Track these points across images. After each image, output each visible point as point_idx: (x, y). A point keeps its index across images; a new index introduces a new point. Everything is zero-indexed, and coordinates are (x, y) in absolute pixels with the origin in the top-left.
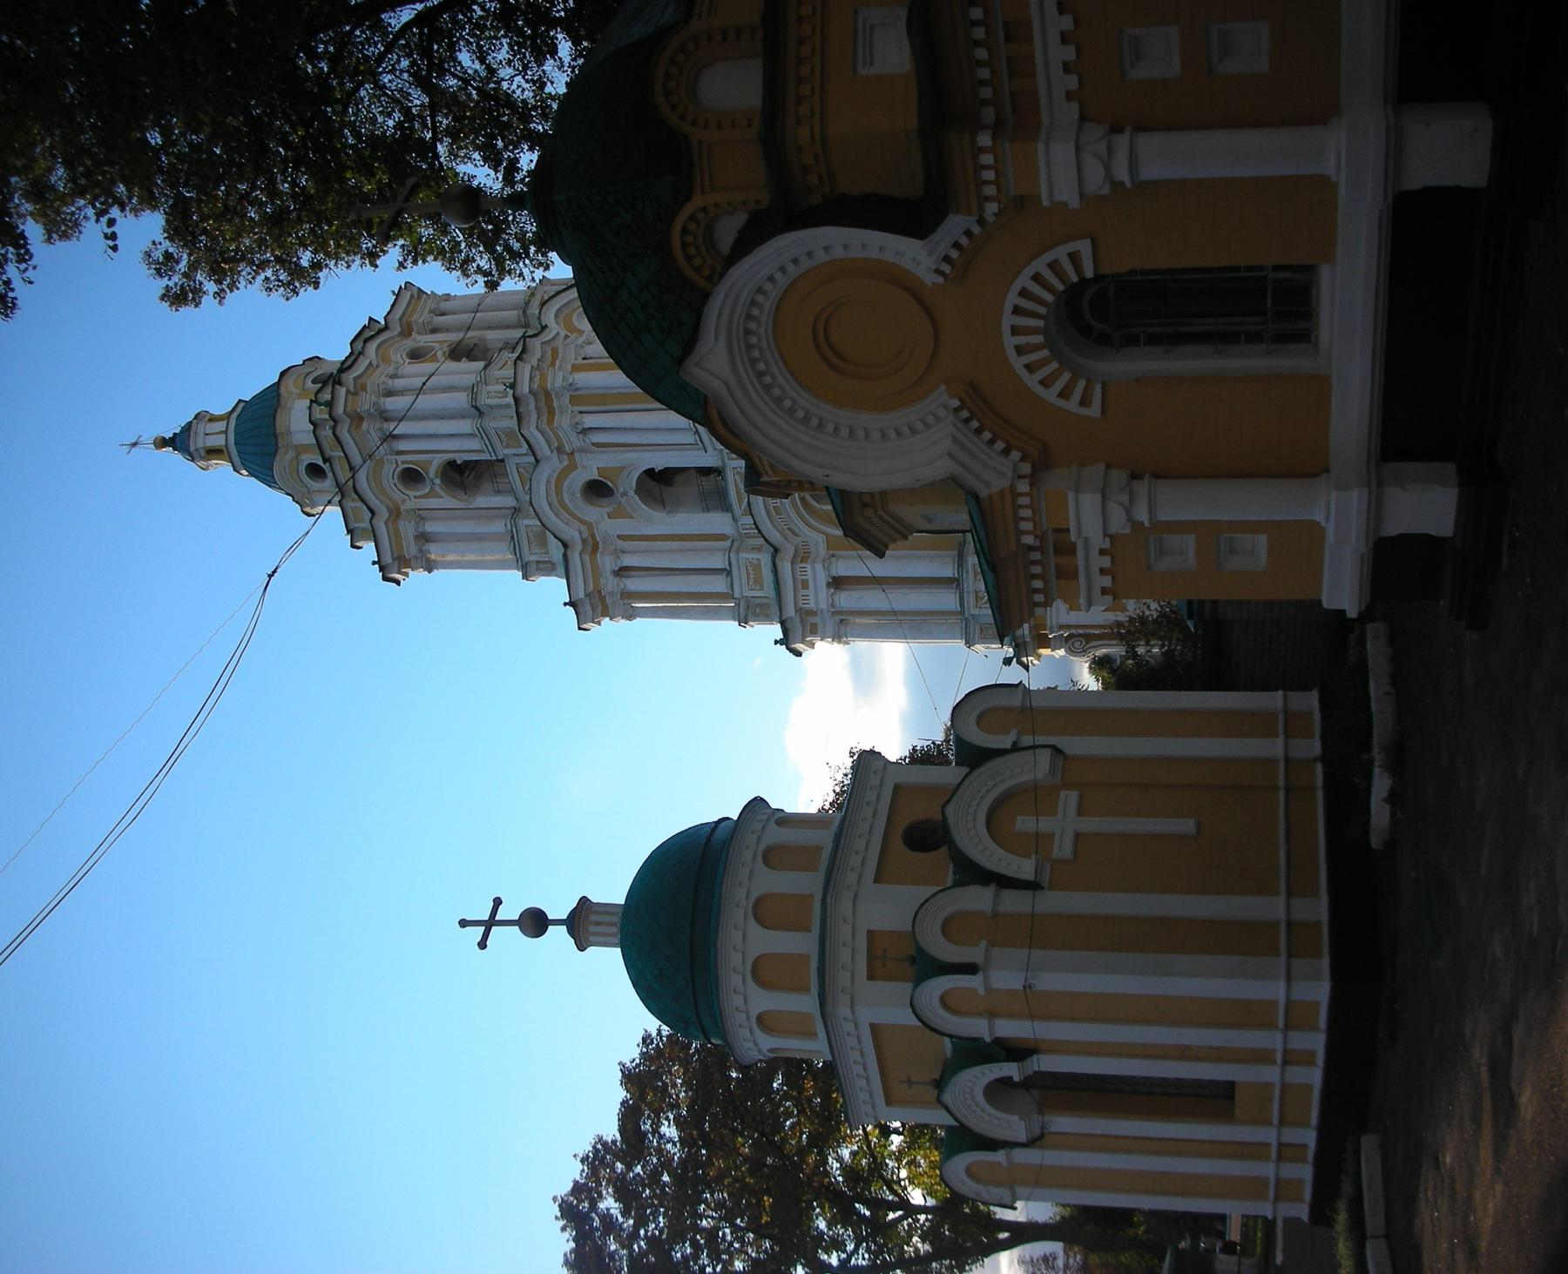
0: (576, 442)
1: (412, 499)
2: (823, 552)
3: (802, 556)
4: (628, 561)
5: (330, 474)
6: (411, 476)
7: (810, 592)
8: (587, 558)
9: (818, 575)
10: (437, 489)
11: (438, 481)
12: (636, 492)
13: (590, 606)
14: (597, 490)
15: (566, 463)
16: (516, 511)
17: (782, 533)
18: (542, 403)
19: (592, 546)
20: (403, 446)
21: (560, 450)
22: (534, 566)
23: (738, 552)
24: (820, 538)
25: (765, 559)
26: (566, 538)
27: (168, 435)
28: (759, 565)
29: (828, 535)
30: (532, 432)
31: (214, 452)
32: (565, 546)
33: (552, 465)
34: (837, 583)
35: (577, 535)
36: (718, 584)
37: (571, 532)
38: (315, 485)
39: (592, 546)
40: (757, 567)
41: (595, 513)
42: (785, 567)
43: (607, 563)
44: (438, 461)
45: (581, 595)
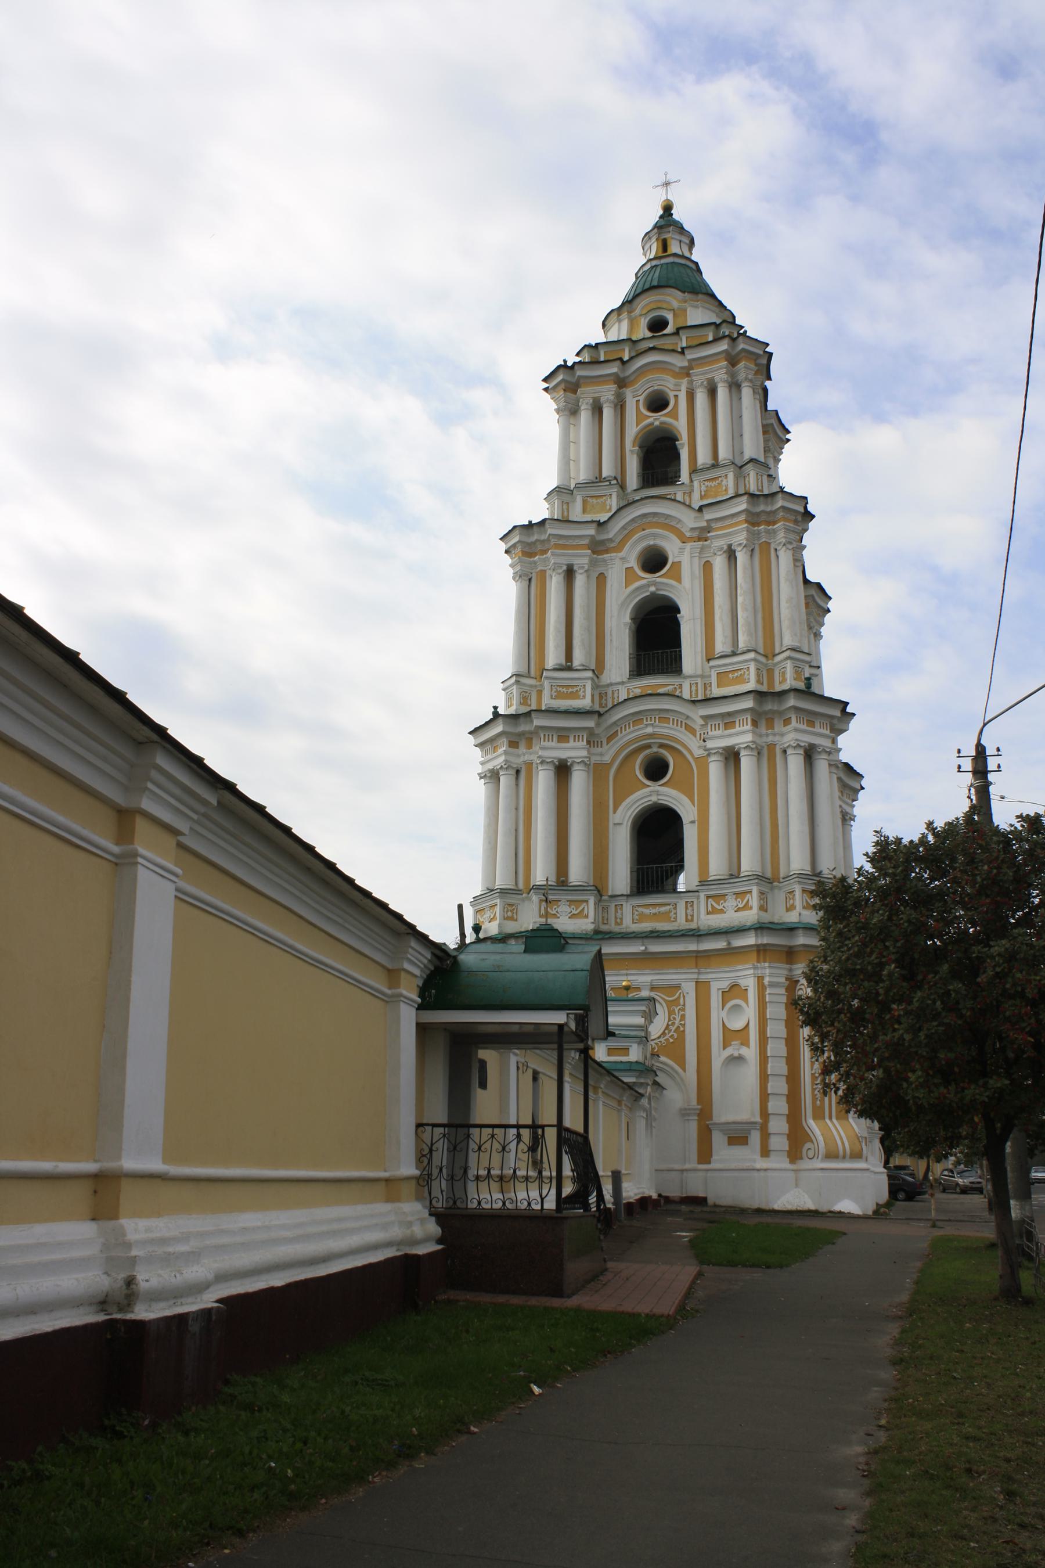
0: (723, 543)
1: (635, 400)
2: (595, 759)
3: (592, 740)
4: (580, 581)
6: (658, 403)
7: (554, 744)
9: (574, 751)
11: (657, 423)
12: (653, 594)
13: (527, 542)
14: (654, 561)
15: (688, 534)
16: (622, 486)
17: (615, 723)
19: (598, 547)
20: (701, 399)
23: (592, 679)
24: (607, 759)
25: (585, 702)
27: (676, 214)
28: (578, 698)
30: (742, 505)
31: (665, 246)
32: (600, 524)
33: (689, 521)
34: (562, 770)
35: (611, 535)
36: (553, 656)
37: (614, 530)
38: (644, 322)
39: (598, 547)
40: (574, 696)
41: (632, 555)
42: (590, 723)
43: (581, 560)
44: (681, 426)
45: (550, 531)
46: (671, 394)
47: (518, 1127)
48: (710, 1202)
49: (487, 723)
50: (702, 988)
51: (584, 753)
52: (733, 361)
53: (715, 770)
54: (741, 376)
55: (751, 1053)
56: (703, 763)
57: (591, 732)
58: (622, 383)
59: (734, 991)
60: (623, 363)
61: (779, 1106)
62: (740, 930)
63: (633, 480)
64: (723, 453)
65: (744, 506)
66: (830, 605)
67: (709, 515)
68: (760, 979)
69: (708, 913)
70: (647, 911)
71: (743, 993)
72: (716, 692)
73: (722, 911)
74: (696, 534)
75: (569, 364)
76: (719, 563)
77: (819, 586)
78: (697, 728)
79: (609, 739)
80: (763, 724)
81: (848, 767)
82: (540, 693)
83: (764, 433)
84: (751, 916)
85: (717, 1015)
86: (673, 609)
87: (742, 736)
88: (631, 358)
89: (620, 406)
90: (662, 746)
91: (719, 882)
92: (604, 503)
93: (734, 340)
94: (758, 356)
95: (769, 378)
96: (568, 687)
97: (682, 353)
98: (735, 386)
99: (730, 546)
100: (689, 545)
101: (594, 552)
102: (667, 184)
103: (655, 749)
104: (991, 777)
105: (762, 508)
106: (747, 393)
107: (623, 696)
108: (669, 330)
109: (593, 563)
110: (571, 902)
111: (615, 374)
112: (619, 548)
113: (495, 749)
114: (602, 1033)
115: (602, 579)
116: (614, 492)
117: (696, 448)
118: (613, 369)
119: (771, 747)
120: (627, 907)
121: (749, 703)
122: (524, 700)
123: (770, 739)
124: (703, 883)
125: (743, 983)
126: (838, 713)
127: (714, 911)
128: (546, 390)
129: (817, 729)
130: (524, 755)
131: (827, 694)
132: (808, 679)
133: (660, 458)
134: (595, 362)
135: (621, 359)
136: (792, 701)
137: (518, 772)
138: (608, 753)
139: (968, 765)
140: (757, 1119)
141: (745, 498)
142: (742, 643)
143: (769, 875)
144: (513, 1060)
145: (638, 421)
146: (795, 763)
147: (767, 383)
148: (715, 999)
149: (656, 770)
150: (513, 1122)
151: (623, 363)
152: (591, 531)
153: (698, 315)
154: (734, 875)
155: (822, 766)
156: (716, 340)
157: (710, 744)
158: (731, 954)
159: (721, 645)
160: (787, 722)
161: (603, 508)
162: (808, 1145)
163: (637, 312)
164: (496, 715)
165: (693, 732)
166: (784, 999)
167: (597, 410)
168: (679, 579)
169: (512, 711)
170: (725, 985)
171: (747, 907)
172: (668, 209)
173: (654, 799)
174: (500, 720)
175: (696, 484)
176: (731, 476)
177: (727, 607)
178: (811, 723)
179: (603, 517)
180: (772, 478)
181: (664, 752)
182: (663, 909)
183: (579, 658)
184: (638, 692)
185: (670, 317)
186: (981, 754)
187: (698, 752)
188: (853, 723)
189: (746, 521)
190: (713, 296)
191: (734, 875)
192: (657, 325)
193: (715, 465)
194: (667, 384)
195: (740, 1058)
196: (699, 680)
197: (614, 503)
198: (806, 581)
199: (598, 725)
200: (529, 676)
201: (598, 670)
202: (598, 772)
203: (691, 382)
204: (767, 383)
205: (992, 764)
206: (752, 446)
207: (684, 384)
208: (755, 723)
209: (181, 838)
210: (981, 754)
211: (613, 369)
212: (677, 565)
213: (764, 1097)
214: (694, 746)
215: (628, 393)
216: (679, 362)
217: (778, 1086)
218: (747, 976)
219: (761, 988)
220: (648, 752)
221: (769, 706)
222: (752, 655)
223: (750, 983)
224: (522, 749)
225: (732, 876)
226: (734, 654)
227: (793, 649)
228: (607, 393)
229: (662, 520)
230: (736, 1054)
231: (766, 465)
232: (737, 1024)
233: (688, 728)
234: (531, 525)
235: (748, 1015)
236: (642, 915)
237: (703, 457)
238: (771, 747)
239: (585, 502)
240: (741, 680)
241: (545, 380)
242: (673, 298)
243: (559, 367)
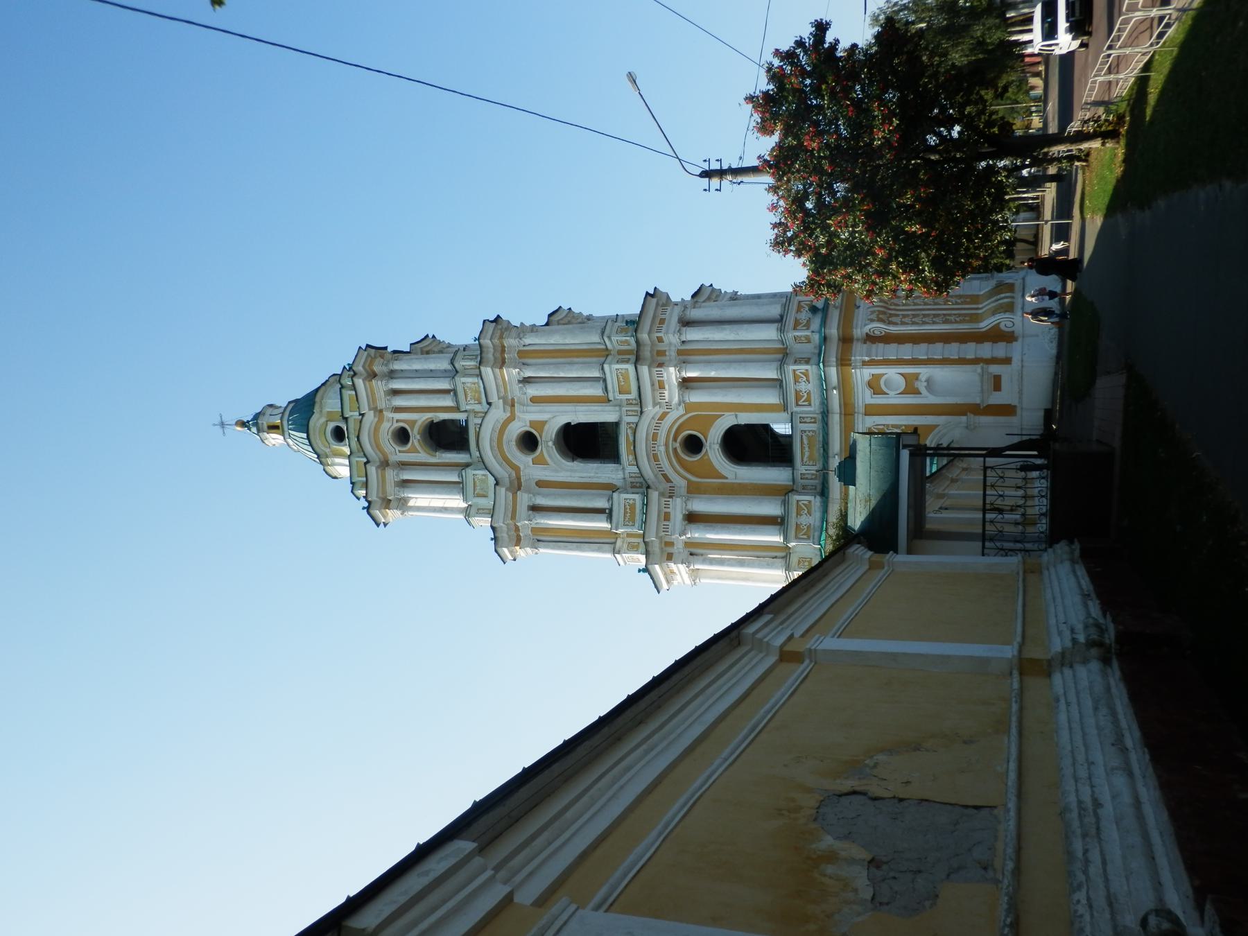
0: (516, 387)
2: (684, 491)
4: (541, 501)
6: (402, 436)
8: (510, 495)
9: (678, 509)
10: (416, 444)
14: (529, 442)
16: (467, 465)
18: (498, 355)
19: (516, 486)
20: (400, 402)
21: (504, 399)
22: (473, 511)
24: (684, 483)
26: (499, 476)
29: (690, 483)
30: (487, 371)
32: (497, 484)
33: (498, 414)
36: (602, 524)
39: (516, 486)
40: (633, 507)
41: (524, 460)
43: (524, 499)
46: (397, 425)
47: (985, 469)
48: (1049, 406)
49: (652, 578)
50: (870, 411)
51: (678, 500)
52: (374, 375)
53: (696, 397)
54: (385, 369)
55: (924, 372)
56: (689, 407)
57: (662, 495)
58: (385, 464)
59: (874, 385)
60: (368, 462)
61: (971, 350)
62: (823, 381)
63: (460, 457)
64: (444, 385)
65: (489, 369)
66: (565, 307)
67: (494, 398)
68: (864, 363)
70: (807, 454)
71: (876, 378)
72: (634, 395)
73: (809, 394)
74: (508, 408)
75: (366, 504)
76: (532, 391)
77: (550, 316)
78: (662, 411)
79: (668, 480)
80: (661, 359)
81: (694, 295)
82: (629, 535)
83: (428, 353)
85: (893, 399)
86: (567, 426)
87: (672, 375)
88: (365, 455)
89: (403, 465)
90: (675, 439)
91: (784, 396)
92: (482, 480)
93: (355, 374)
94: (369, 355)
95: (386, 348)
96: (625, 513)
97: (363, 415)
98: (392, 375)
99: (520, 382)
100: (517, 413)
101: (519, 489)
102: (222, 424)
103: (677, 445)
104: (725, 167)
105: (490, 356)
106: (397, 366)
107: (635, 469)
109: (529, 491)
110: (798, 514)
111: (377, 468)
112: (517, 469)
113: (672, 572)
114: (915, 437)
115: (541, 484)
116: (470, 472)
117: (441, 408)
118: (372, 470)
119: (680, 352)
120: (801, 468)
121: (644, 370)
122: (633, 548)
123: (673, 354)
124: (785, 408)
125: (867, 377)
126: (654, 301)
127: (809, 400)
128: (385, 525)
129: (666, 316)
130: (679, 547)
131: (637, 311)
132: (627, 322)
133: (448, 436)
134: (366, 485)
135: (365, 464)
136: (644, 336)
137: (691, 554)
138: (680, 483)
139: (715, 182)
140: (978, 368)
141: (482, 368)
142: (597, 374)
143: (780, 356)
144: (932, 515)
145: (417, 451)
147: (390, 350)
148: (880, 400)
149: (693, 445)
150: (981, 516)
151: (368, 462)
152: (502, 491)
153: (330, 403)
154: (779, 384)
155: (695, 314)
156: (354, 387)
157: (676, 400)
159: (596, 391)
160: (660, 340)
161: (484, 481)
162: (1002, 326)
163: (327, 450)
164: (646, 570)
165: (664, 415)
166: (881, 345)
167: (405, 483)
168: (544, 423)
169: (643, 558)
170: (868, 392)
171: (806, 374)
172: (243, 424)
173: (717, 447)
174: (650, 567)
175: (468, 408)
176: (463, 380)
177: (568, 385)
178: (662, 321)
179: (491, 480)
180: (465, 348)
181: (679, 439)
182: (805, 441)
183: (601, 503)
184: (631, 458)
185: (331, 425)
186: (707, 174)
187: (681, 411)
188: (662, 289)
189: (501, 368)
190: (317, 390)
191: (779, 384)
192: (339, 435)
193: (455, 391)
194: (388, 428)
195: (928, 381)
196: (624, 409)
197: (480, 473)
198: (547, 324)
199: (656, 489)
200: (615, 543)
201: (612, 488)
202: (694, 490)
203: (387, 409)
204: (390, 350)
205: (715, 166)
206: (442, 364)
207: (388, 414)
208: (661, 365)
209: (797, 635)
210: (707, 174)
211: (372, 470)
212: (532, 423)
213: (962, 361)
214: (676, 414)
215: (393, 458)
216: (370, 417)
217: (953, 350)
218: (861, 375)
219: (872, 363)
220: (679, 450)
221: (646, 353)
222: (606, 366)
223: (867, 373)
224: (674, 550)
225: (781, 386)
226: (605, 380)
227: (603, 333)
228: (391, 475)
229: (496, 435)
231: (455, 353)
233: (662, 417)
234: (495, 539)
235: (893, 375)
236: (810, 458)
237: (448, 402)
238: (680, 352)
239: (479, 496)
240: (626, 376)
241: (378, 525)
242: (316, 421)
243: (369, 513)
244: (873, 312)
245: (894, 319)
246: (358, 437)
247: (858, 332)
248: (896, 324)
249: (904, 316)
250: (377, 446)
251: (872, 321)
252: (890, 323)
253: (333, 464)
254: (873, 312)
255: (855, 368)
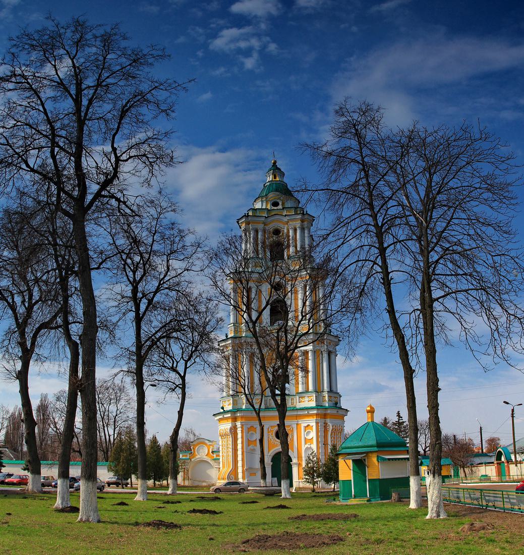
5: (275, 208)
58: (265, 224)
68: (317, 423)
69: (299, 402)
84: (313, 404)
98: (303, 229)
108: (280, 207)
125: (311, 424)
146: (325, 356)
154: (307, 391)
158: (309, 415)
170: (306, 425)
185: (280, 203)
230: (309, 446)
232: (309, 437)
235: (313, 434)
244: (336, 426)
245: (333, 434)
246: (275, 214)
247: (328, 421)
248: (331, 435)
249: (334, 438)
250: (272, 221)
251: (333, 426)
252: (332, 433)
253: (262, 201)
254: (336, 426)
255: (316, 420)
